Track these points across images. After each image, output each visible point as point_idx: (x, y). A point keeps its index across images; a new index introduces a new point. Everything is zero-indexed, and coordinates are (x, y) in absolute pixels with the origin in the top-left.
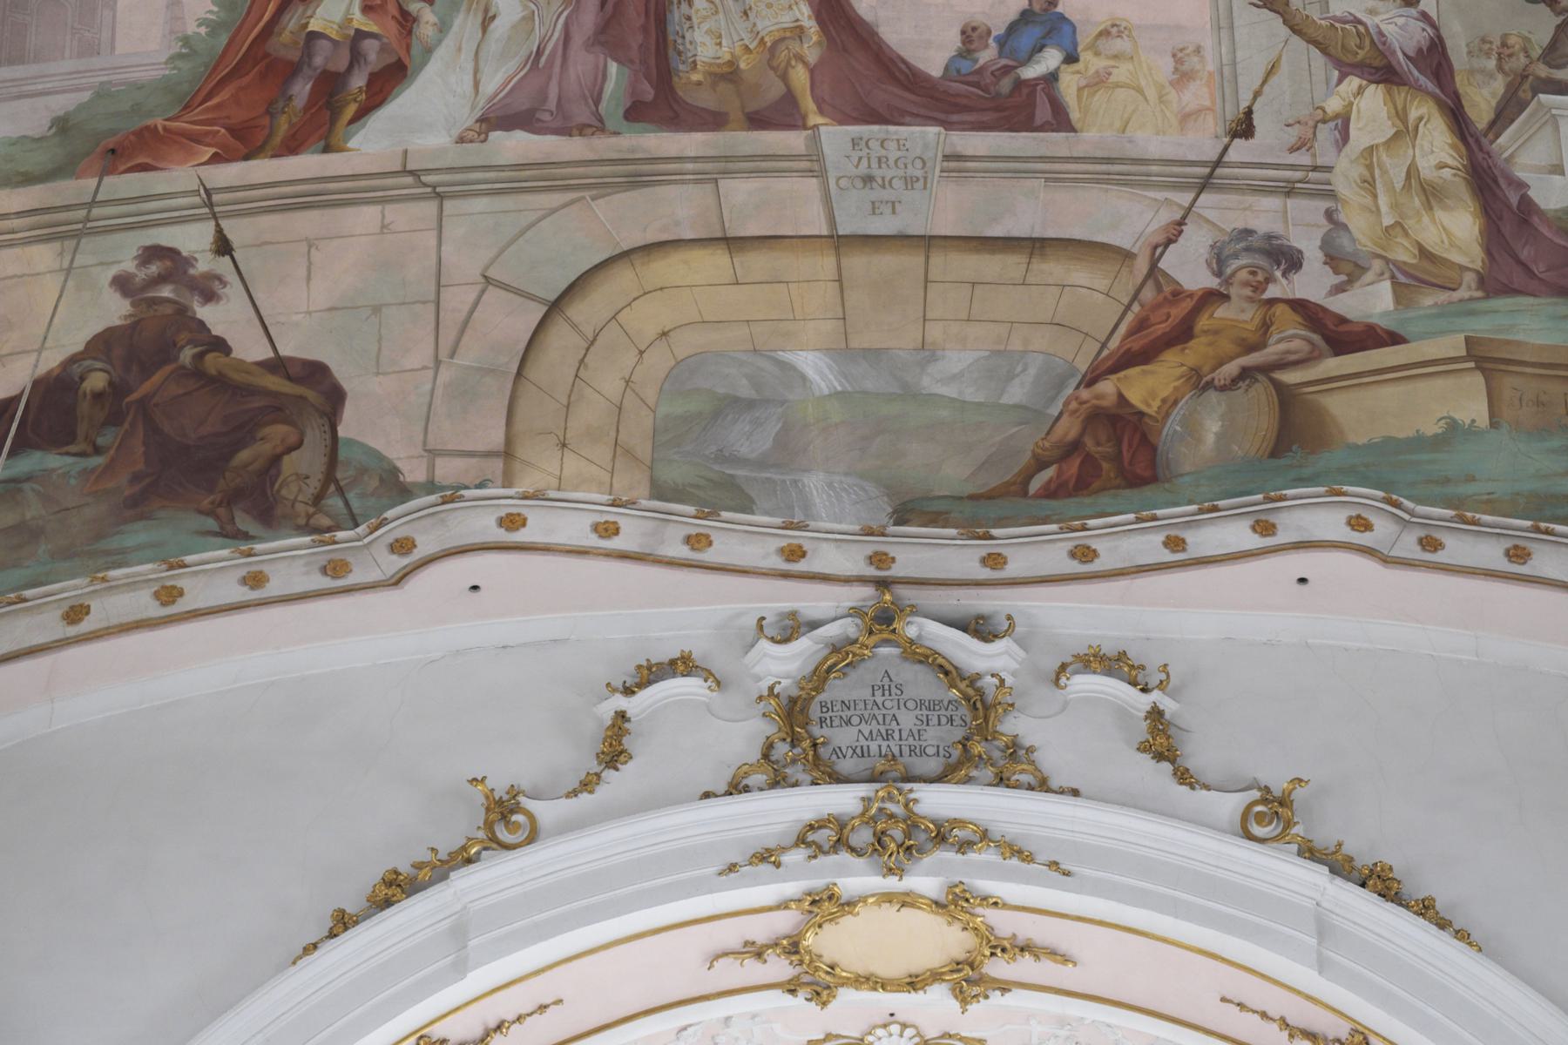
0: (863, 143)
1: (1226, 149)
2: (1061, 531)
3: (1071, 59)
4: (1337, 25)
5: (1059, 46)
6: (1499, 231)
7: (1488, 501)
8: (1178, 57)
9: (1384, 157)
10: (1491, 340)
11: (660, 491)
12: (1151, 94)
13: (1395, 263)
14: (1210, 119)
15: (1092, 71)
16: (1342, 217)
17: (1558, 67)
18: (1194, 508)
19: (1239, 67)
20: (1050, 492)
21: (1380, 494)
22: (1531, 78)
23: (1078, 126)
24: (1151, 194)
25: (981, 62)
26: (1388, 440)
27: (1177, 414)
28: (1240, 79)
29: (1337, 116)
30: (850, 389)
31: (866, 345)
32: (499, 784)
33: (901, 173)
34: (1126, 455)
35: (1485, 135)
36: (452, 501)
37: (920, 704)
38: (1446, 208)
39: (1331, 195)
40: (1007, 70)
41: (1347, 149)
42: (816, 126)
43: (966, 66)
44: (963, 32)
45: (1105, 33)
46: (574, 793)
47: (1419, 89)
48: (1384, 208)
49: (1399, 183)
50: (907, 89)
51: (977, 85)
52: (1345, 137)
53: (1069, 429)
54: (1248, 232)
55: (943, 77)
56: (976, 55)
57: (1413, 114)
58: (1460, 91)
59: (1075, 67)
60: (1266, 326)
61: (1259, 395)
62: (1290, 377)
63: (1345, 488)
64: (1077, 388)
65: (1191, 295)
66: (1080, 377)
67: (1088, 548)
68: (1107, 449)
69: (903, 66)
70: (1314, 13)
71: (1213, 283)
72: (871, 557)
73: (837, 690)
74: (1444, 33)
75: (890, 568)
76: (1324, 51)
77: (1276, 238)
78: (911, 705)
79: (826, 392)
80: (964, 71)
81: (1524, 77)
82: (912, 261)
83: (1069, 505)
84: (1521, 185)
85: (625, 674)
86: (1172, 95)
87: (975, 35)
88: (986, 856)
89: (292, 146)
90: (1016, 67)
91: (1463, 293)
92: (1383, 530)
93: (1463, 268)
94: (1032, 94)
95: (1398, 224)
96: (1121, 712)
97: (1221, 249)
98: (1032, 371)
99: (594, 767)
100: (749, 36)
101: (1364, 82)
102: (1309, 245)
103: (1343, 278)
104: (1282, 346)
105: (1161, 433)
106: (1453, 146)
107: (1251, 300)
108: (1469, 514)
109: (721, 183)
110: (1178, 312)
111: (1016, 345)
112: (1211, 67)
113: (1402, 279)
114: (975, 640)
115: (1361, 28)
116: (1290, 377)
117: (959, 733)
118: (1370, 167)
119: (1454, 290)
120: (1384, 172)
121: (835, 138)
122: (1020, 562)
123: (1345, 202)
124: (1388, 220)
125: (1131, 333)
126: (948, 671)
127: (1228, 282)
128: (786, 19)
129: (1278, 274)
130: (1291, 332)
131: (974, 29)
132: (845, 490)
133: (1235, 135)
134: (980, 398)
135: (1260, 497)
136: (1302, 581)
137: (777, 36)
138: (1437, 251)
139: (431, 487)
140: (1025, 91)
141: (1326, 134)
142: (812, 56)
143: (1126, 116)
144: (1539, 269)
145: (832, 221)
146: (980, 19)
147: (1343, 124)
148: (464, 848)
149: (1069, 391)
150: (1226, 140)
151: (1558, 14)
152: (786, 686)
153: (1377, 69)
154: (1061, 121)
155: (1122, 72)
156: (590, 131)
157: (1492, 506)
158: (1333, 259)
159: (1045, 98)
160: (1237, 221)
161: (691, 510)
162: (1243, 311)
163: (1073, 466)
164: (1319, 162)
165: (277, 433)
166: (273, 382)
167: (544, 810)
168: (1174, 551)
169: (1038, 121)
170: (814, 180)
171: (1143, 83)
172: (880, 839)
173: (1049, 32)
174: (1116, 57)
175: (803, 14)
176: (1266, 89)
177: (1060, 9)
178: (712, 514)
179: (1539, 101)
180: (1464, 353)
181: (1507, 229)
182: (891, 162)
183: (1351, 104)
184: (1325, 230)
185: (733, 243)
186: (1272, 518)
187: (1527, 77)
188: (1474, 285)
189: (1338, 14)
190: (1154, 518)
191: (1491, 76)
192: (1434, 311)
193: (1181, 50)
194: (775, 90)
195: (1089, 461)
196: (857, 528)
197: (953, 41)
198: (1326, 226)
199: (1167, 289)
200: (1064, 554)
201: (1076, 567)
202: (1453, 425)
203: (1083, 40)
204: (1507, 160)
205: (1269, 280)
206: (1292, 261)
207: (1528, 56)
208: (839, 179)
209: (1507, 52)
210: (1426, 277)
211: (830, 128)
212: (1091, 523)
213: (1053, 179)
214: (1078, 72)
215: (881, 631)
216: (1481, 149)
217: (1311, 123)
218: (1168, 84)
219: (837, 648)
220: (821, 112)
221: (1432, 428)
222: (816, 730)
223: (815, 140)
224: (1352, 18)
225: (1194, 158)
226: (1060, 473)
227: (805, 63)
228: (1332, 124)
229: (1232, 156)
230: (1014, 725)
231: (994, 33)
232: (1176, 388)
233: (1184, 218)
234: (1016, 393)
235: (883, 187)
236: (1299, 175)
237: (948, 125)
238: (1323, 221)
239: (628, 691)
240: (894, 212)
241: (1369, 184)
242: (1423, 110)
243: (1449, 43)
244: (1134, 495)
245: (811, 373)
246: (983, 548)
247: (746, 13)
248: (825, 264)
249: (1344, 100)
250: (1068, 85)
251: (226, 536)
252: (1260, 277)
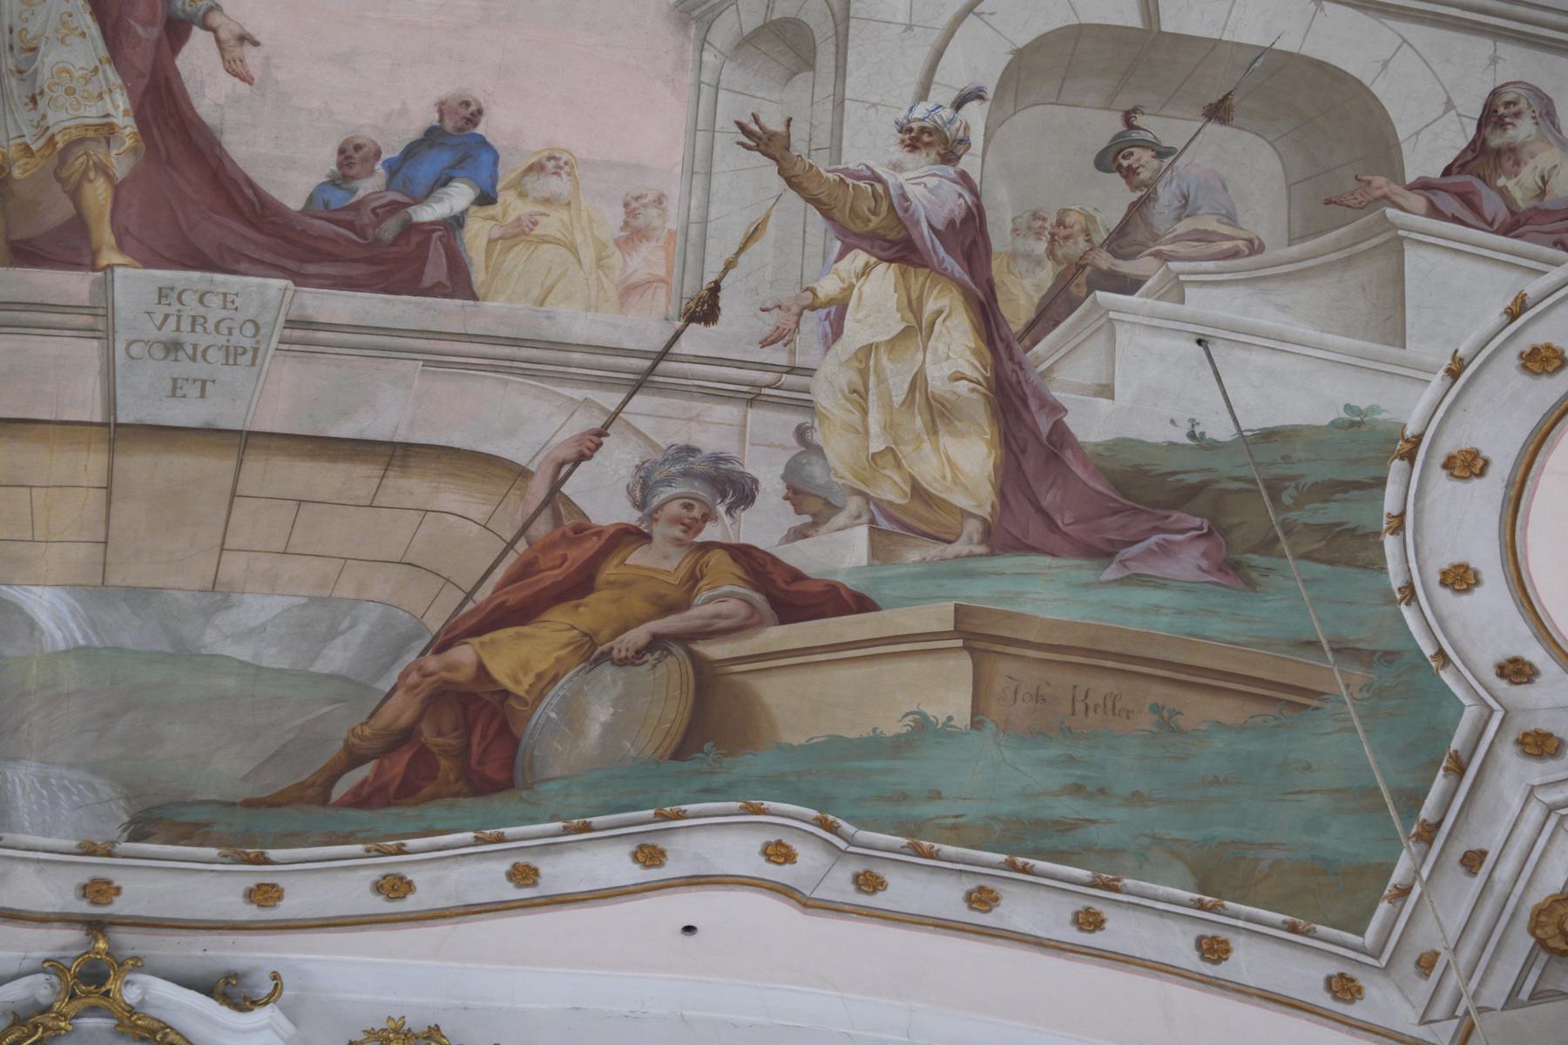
0: (175, 295)
1: (676, 336)
2: (368, 854)
3: (486, 199)
4: (849, 181)
5: (472, 180)
6: (1019, 465)
7: (954, 827)
8: (631, 209)
9: (884, 360)
10: (988, 610)
12: (588, 255)
13: (878, 503)
14: (662, 293)
15: (511, 218)
16: (817, 438)
17: (1126, 257)
18: (558, 825)
19: (711, 226)
21: (813, 813)
22: (1089, 269)
23: (479, 291)
24: (567, 391)
25: (361, 194)
26: (835, 741)
27: (555, 694)
28: (710, 242)
29: (830, 302)
30: (96, 643)
31: (131, 582)
33: (222, 340)
34: (476, 749)
35: (1020, 340)
38: (955, 433)
39: (808, 407)
40: (394, 208)
41: (838, 347)
42: (111, 267)
43: (337, 198)
44: (342, 151)
45: (537, 168)
47: (944, 273)
48: (874, 426)
49: (899, 395)
50: (252, 225)
51: (350, 226)
52: (837, 330)
53: (402, 710)
54: (690, 450)
55: (304, 211)
56: (355, 184)
57: (931, 306)
58: (996, 280)
59: (490, 210)
60: (693, 579)
61: (672, 671)
62: (715, 650)
63: (767, 804)
64: (423, 653)
65: (599, 532)
66: (428, 639)
67: (402, 878)
68: (450, 740)
69: (249, 192)
70: (821, 163)
72: (85, 887)
74: (986, 202)
75: (110, 903)
76: (827, 214)
77: (727, 460)
79: (62, 646)
80: (333, 206)
81: (1081, 267)
82: (215, 467)
83: (382, 819)
84: (1057, 409)
86: (616, 258)
87: (357, 156)
90: (407, 205)
91: (960, 547)
92: (809, 860)
93: (965, 514)
94: (424, 245)
95: (889, 449)
97: (649, 473)
98: (363, 628)
100: (34, 131)
101: (873, 260)
102: (769, 478)
103: (807, 519)
104: (711, 608)
105: (528, 720)
106: (976, 353)
107: (679, 542)
108: (926, 844)
110: (578, 554)
111: (347, 590)
112: (673, 224)
113: (884, 524)
114: (225, 1009)
115: (879, 188)
116: (715, 650)
118: (864, 374)
119: (949, 542)
120: (882, 380)
122: (300, 899)
123: (824, 418)
124: (876, 446)
125: (510, 580)
127: (652, 518)
128: (91, 113)
129: (721, 509)
130: (726, 589)
131: (358, 148)
132: (65, 789)
133: (692, 317)
134: (283, 664)
135: (650, 813)
136: (689, 929)
137: (75, 134)
138: (935, 489)
140: (415, 239)
141: (812, 324)
142: (121, 167)
143: (548, 283)
144: (1064, 520)
145: (111, 403)
146: (367, 134)
147: (836, 313)
149: (411, 657)
150: (679, 324)
151: (1135, 188)
153: (893, 243)
154: (459, 283)
155: (552, 223)
157: (957, 833)
158: (796, 494)
159: (442, 251)
160: (678, 435)
162: (666, 557)
163: (398, 766)
164: (799, 361)
168: (519, 886)
169: (427, 280)
170: (95, 343)
171: (579, 238)
173: (460, 162)
174: (547, 201)
175: (116, 107)
176: (743, 258)
177: (480, 130)
179: (1095, 301)
180: (950, 627)
181: (1030, 465)
182: (210, 326)
183: (852, 287)
184: (785, 458)
186: (661, 843)
187: (1084, 267)
188: (976, 538)
189: (852, 166)
190: (500, 839)
191: (1039, 263)
192: (919, 569)
193: (637, 199)
194: (62, 210)
195: (424, 760)
196: (72, 844)
197: (327, 161)
198: (795, 447)
199: (568, 522)
200: (366, 886)
201: (381, 905)
202: (922, 725)
203: (506, 175)
204: (1043, 375)
205: (708, 516)
206: (741, 492)
207: (1088, 241)
208: (130, 344)
209: (1063, 232)
210: (924, 528)
211: (131, 271)
212: (412, 843)
213: (435, 363)
214: (493, 218)
215: (88, 994)
216: (1011, 358)
217: (795, 309)
218: (611, 243)
220: (121, 247)
221: (893, 727)
223: (106, 287)
224: (868, 173)
225: (632, 346)
226: (378, 772)
227: (110, 177)
228: (822, 312)
229: (684, 346)
231: (385, 156)
232: (558, 660)
233: (606, 426)
234: (337, 658)
235: (194, 359)
236: (769, 377)
237: (300, 279)
238: (793, 442)
240: (202, 395)
241: (859, 396)
242: (944, 302)
243: (990, 217)
244: (477, 805)
245: (44, 619)
246: (252, 876)
247: (33, 100)
248: (91, 463)
249: (843, 281)
250: (477, 236)
252: (697, 512)
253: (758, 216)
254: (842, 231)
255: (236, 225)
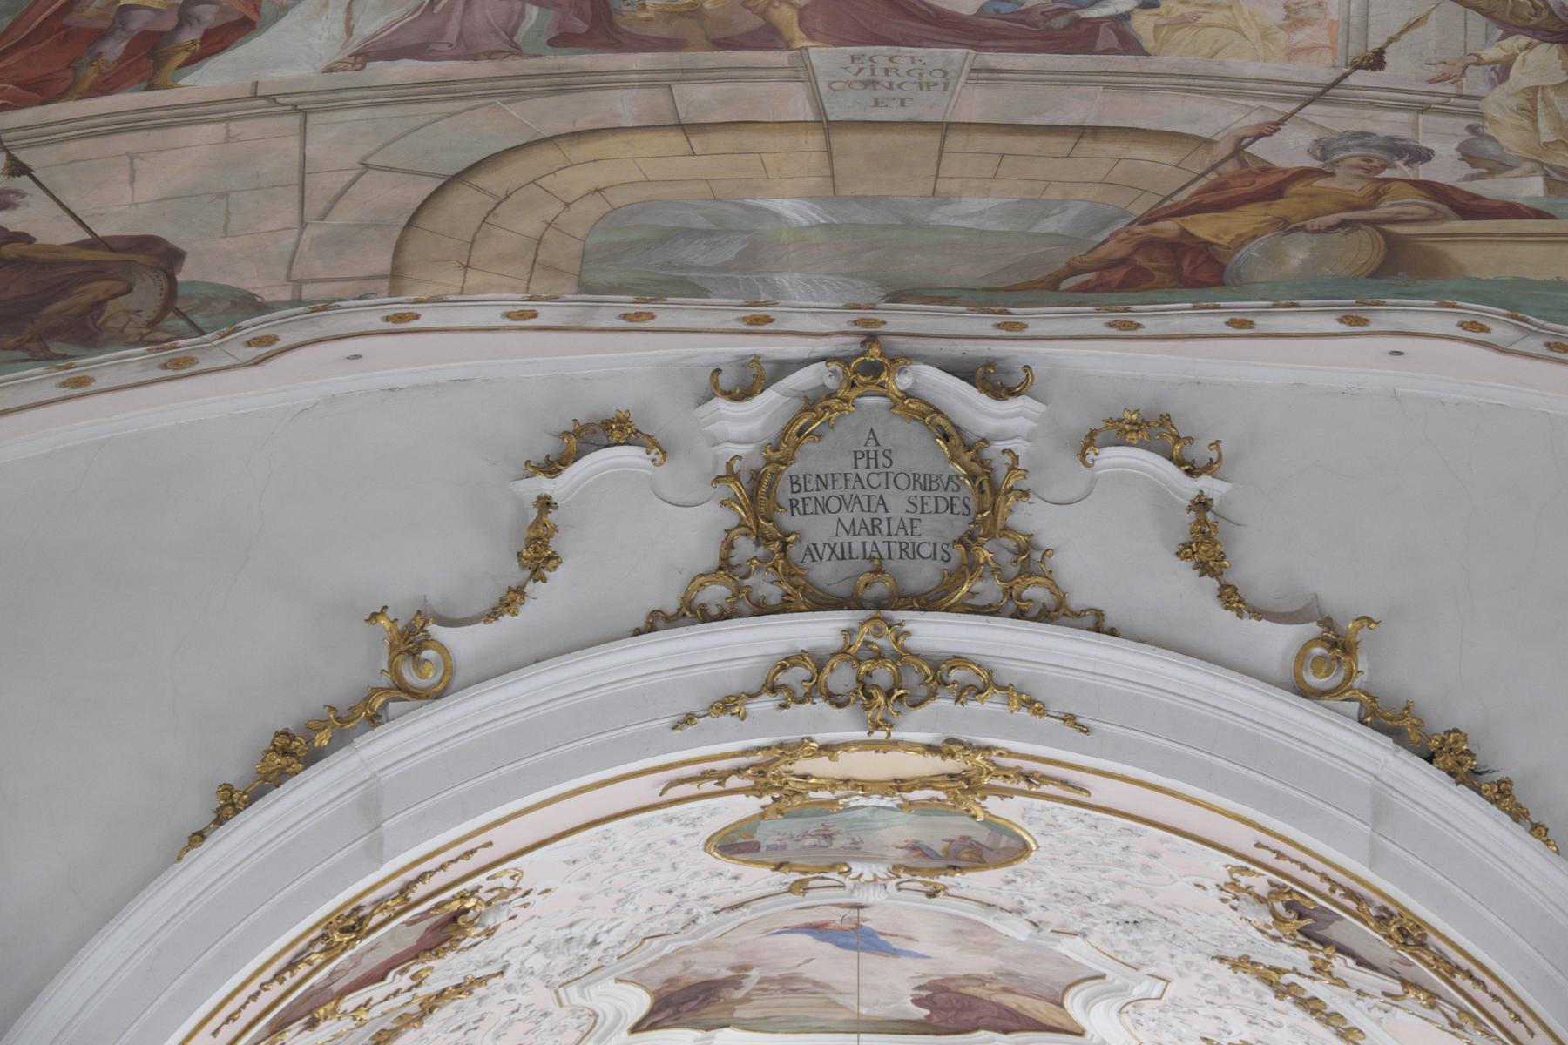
11: (584, 288)
14: (1328, 55)
20: (1084, 288)
24: (1243, 102)
28: (1371, 28)
32: (402, 606)
36: (325, 310)
37: (914, 480)
46: (492, 615)
51: (1022, 22)
71: (1316, 164)
73: (812, 460)
78: (902, 481)
85: (547, 447)
88: (992, 705)
89: (105, 87)
96: (1161, 495)
99: (516, 575)
109: (676, 89)
114: (984, 396)
117: (960, 525)
121: (825, 57)
126: (950, 434)
139: (297, 302)
148: (366, 702)
152: (748, 454)
153: (1555, 33)
156: (503, 55)
159: (1111, 32)
161: (631, 298)
163: (1119, 274)
165: (98, 288)
166: (88, 255)
167: (462, 642)
169: (1100, 45)
170: (800, 84)
171: (1242, 24)
172: (865, 688)
176: (1405, 37)
178: (659, 298)
183: (1516, 55)
185: (687, 128)
215: (867, 384)
219: (815, 403)
220: (810, 37)
222: (787, 521)
225: (1302, 80)
230: (1030, 517)
234: (1050, 225)
237: (977, 48)
239: (552, 467)
245: (787, 213)
249: (1506, 51)
251: (34, 360)
253: (1418, 14)
254: (1501, 23)
255: (915, 24)
